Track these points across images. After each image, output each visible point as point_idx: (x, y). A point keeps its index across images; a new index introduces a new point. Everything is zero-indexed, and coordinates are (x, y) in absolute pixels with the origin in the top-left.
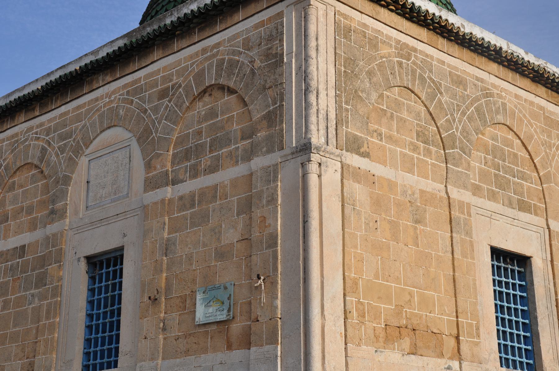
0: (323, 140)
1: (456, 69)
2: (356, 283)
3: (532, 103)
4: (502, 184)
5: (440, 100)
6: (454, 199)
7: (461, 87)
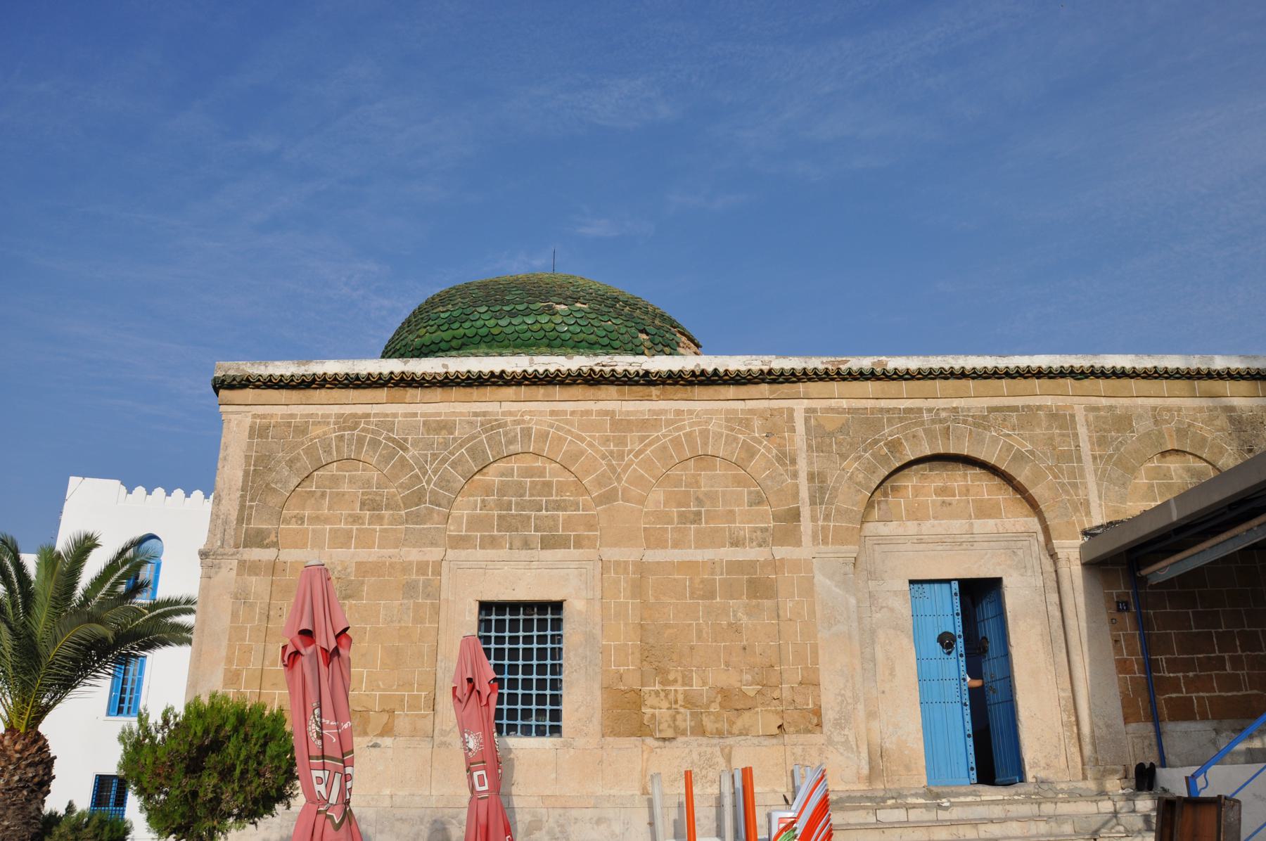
1: (439, 414)
5: (402, 459)
7: (444, 432)
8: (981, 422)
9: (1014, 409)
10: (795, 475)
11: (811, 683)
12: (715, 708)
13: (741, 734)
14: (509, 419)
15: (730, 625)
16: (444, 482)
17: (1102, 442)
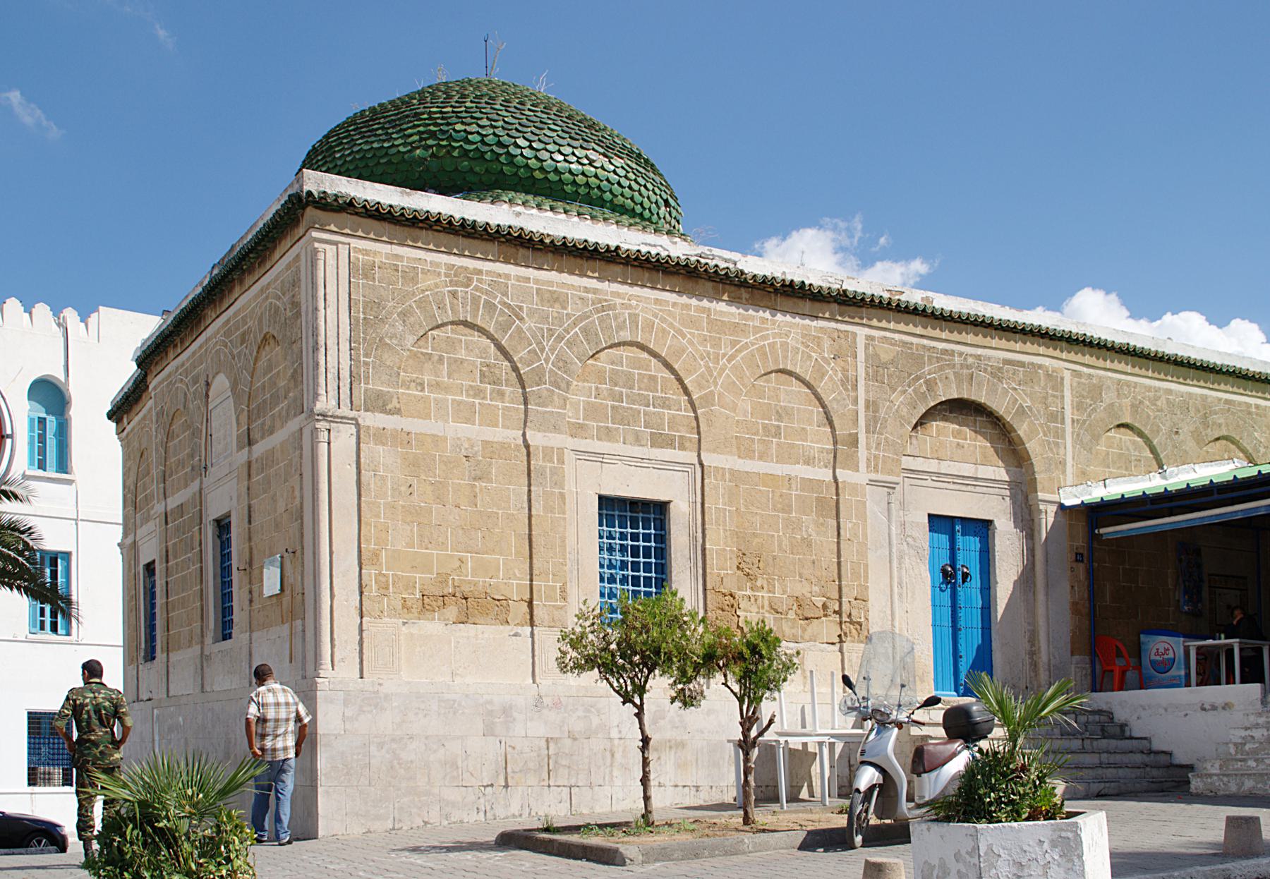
0: (334, 403)
2: (376, 555)
3: (688, 307)
4: (622, 417)
5: (519, 329)
6: (537, 448)
7: (557, 305)
8: (997, 374)
9: (1022, 364)
10: (856, 402)
11: (861, 599)
12: (792, 615)
13: (810, 640)
14: (618, 301)
15: (803, 539)
16: (563, 363)
17: (1079, 407)
